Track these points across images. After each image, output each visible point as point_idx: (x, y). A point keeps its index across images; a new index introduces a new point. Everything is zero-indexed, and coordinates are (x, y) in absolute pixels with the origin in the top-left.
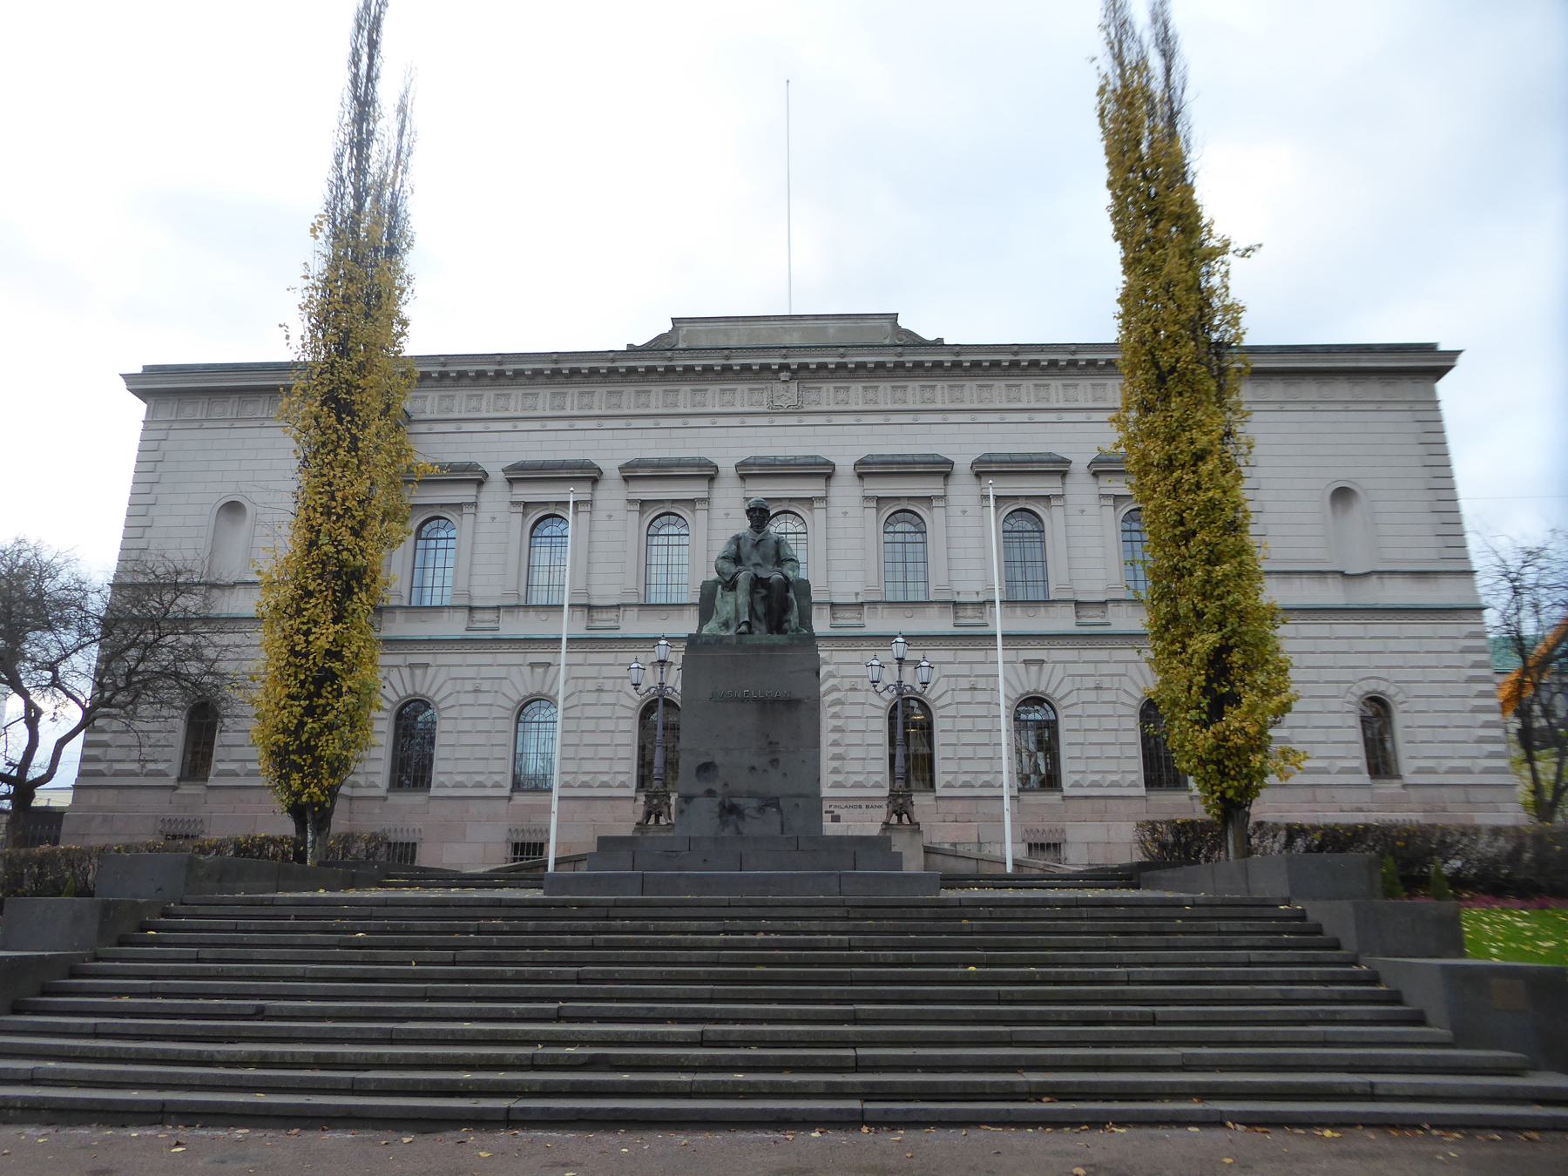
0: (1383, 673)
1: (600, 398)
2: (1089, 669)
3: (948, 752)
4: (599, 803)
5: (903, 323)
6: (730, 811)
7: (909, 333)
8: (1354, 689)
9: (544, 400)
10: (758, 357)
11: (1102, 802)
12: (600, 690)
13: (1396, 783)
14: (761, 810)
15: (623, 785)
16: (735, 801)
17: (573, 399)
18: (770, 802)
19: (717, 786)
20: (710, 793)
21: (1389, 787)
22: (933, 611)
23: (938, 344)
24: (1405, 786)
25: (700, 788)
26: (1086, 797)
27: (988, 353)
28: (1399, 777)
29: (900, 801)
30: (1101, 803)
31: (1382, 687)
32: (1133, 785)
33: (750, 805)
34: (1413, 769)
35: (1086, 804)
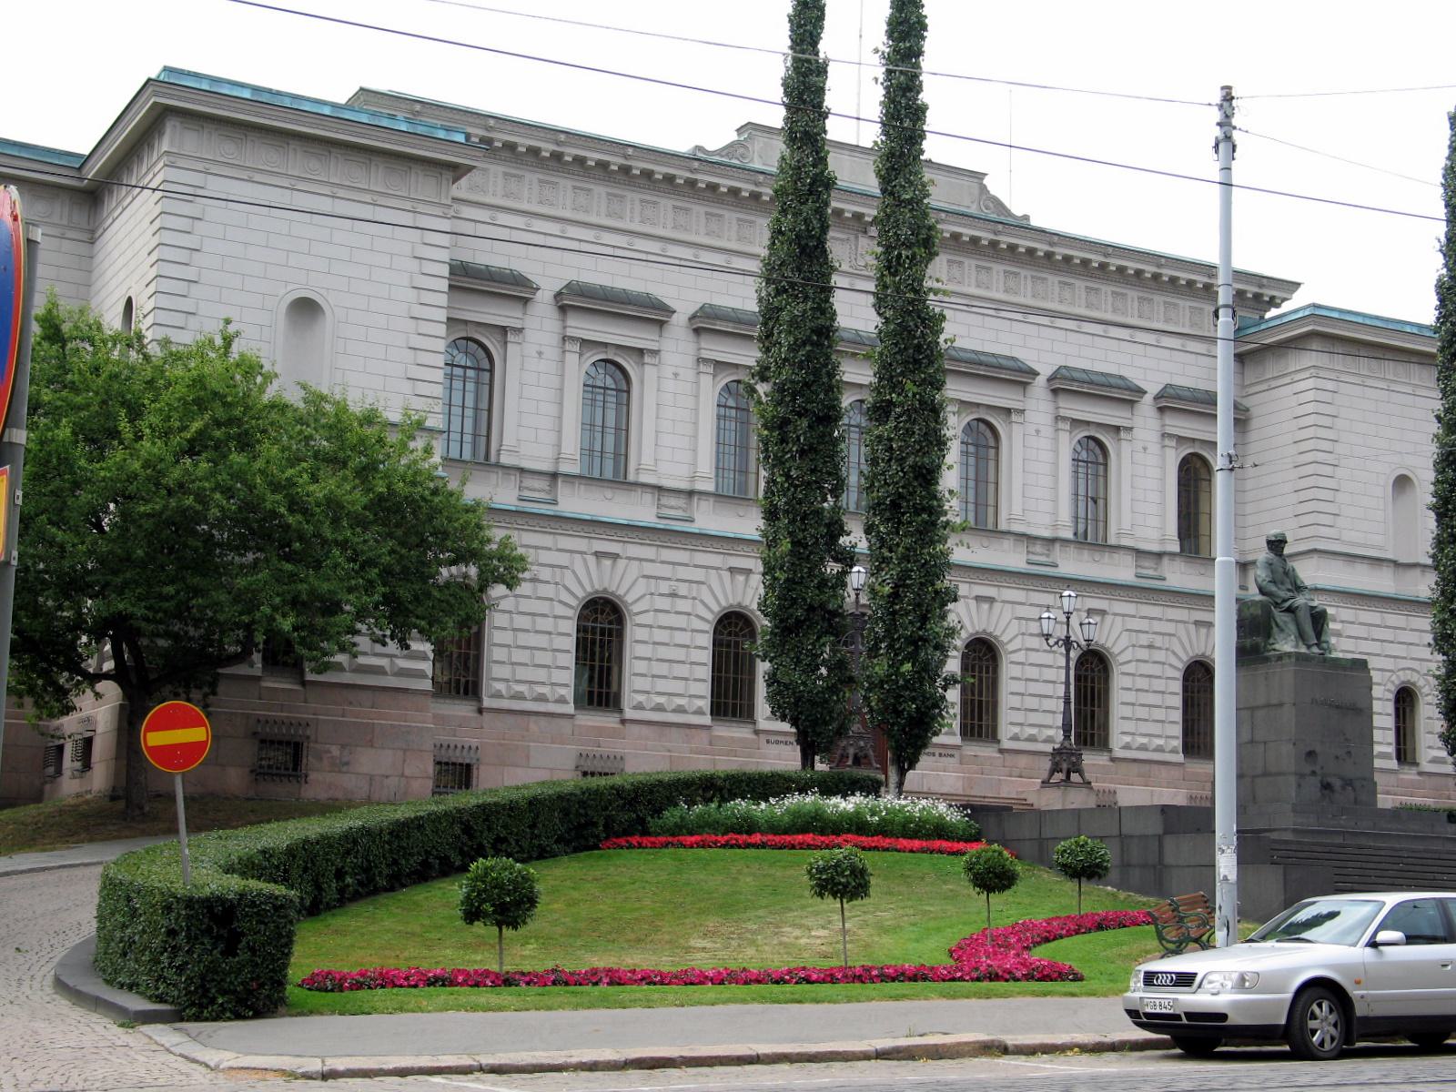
0: (1415, 665)
1: (665, 214)
2: (1144, 625)
3: (1015, 701)
4: (674, 730)
5: (995, 186)
6: (1327, 787)
7: (998, 204)
8: (1394, 678)
9: (598, 201)
10: (854, 203)
11: (1147, 767)
12: (674, 595)
13: (1414, 770)
14: (1343, 788)
15: (699, 712)
16: (1329, 780)
17: (634, 209)
18: (1348, 783)
19: (1317, 769)
20: (1314, 773)
21: (1409, 774)
22: (1008, 543)
23: (1022, 226)
24: (1420, 774)
25: (1308, 769)
26: (1135, 760)
27: (1081, 249)
28: (1415, 764)
29: (1074, 759)
30: (1145, 767)
31: (1414, 677)
32: (1174, 751)
33: (1337, 783)
34: (1429, 758)
35: (1135, 767)
